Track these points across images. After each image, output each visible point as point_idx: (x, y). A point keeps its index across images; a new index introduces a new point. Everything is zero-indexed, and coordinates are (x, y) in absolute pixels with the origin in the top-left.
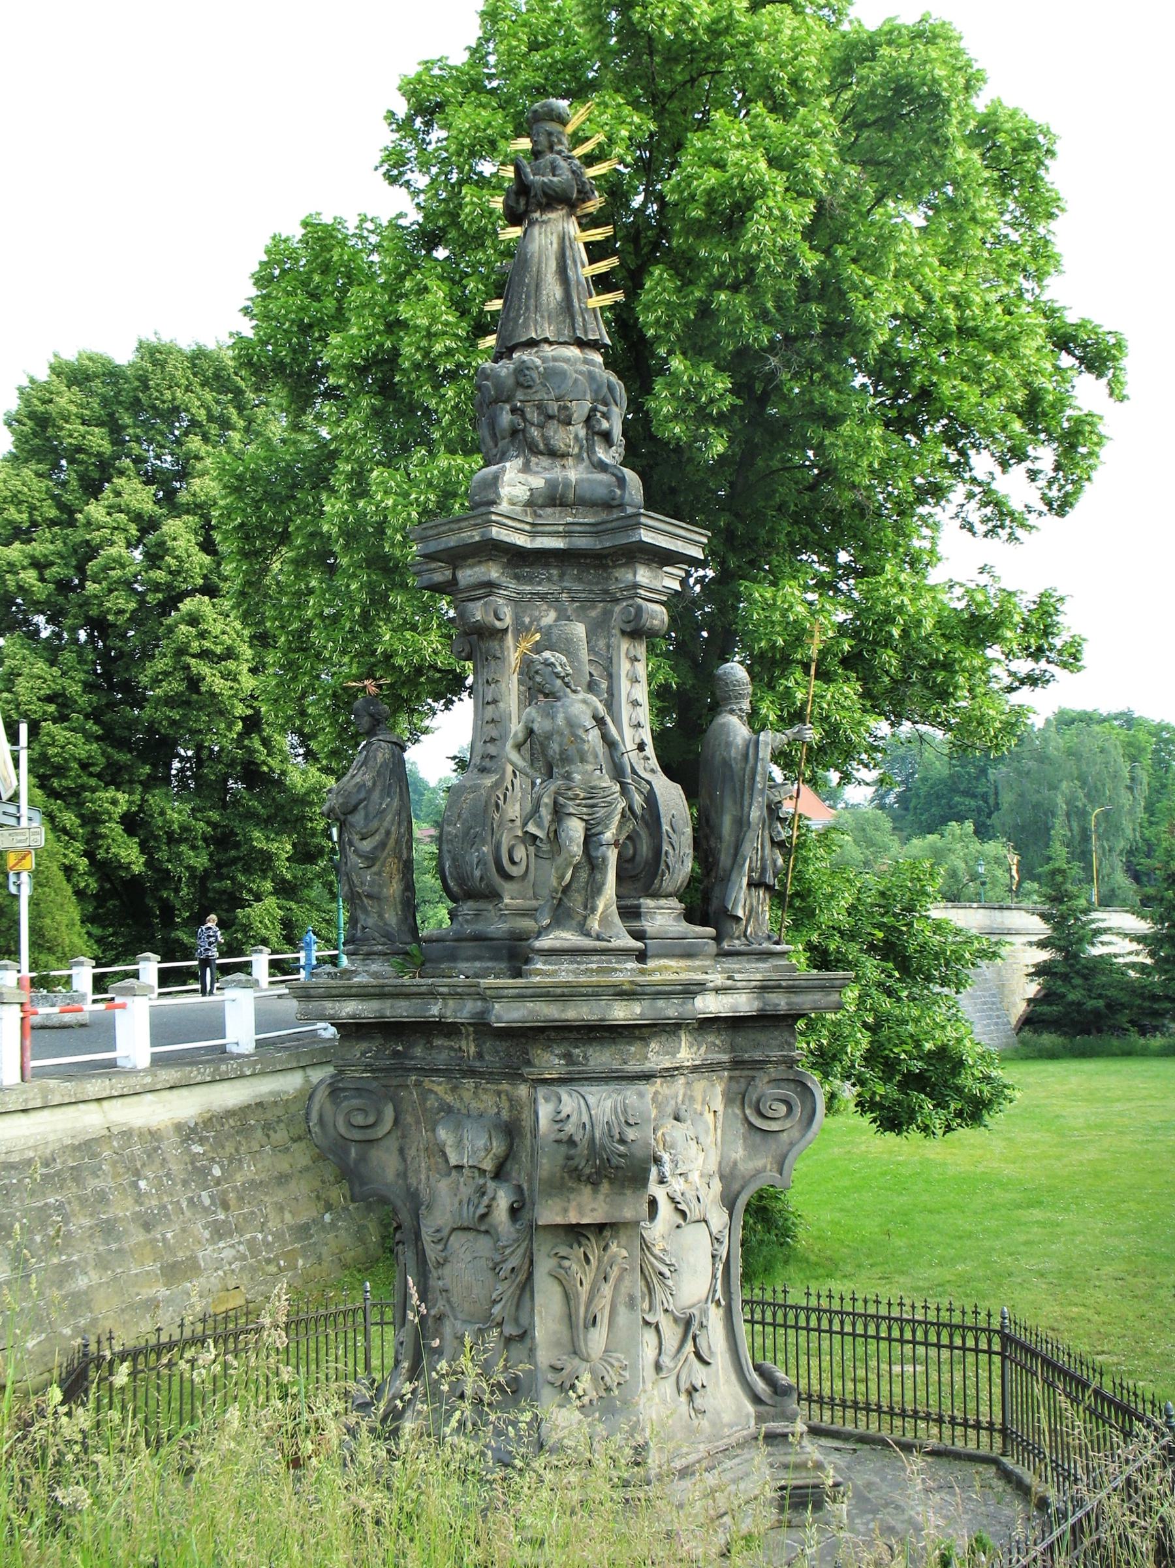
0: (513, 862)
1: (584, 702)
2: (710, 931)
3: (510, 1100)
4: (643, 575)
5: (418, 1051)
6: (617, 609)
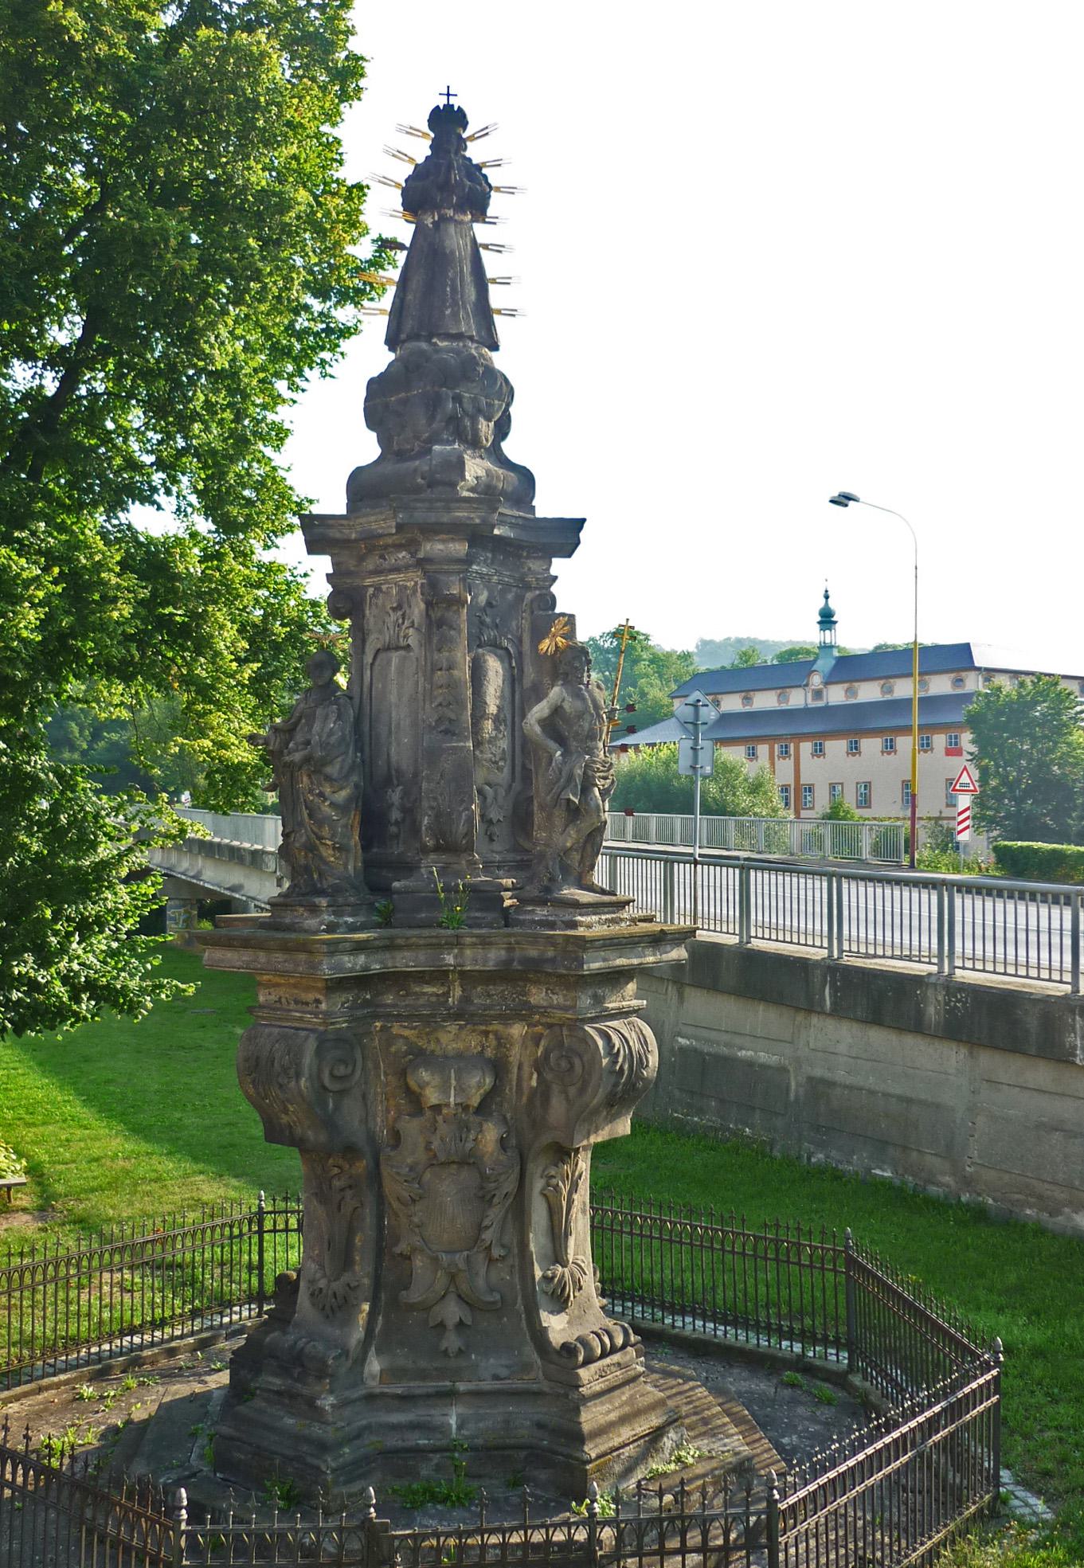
3: (498, 1038)
5: (389, 999)
6: (529, 596)
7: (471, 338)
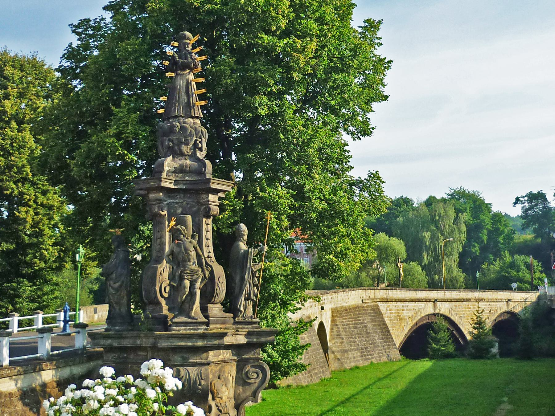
0: (165, 292)
1: (190, 242)
2: (232, 315)
4: (211, 197)
5: (132, 357)
6: (202, 208)
7: (181, 116)
